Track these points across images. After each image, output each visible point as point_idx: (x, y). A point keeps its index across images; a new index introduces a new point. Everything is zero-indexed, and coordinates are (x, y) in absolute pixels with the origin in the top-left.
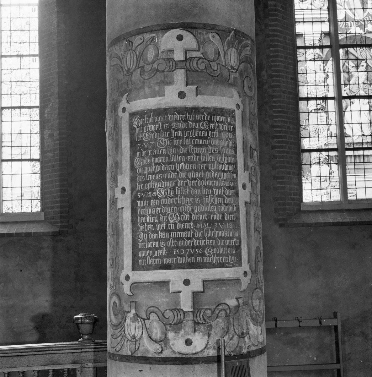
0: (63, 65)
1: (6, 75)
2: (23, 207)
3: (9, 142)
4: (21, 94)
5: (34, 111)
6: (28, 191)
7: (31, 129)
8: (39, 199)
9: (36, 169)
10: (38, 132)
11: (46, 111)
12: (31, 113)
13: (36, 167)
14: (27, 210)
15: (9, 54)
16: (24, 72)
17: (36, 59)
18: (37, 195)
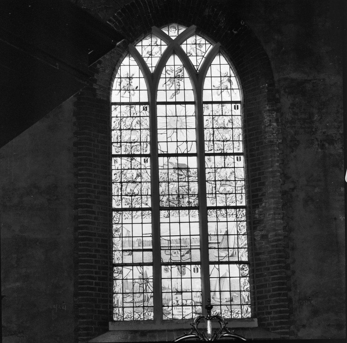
0: (277, 164)
1: (210, 174)
2: (233, 313)
3: (215, 243)
4: (226, 194)
5: (241, 211)
6: (237, 295)
7: (238, 230)
8: (249, 304)
9: (245, 272)
10: (245, 233)
11: (257, 212)
12: (237, 213)
13: (245, 269)
14: (237, 315)
15: (212, 152)
16: (229, 171)
17: (240, 157)
18: (247, 300)
